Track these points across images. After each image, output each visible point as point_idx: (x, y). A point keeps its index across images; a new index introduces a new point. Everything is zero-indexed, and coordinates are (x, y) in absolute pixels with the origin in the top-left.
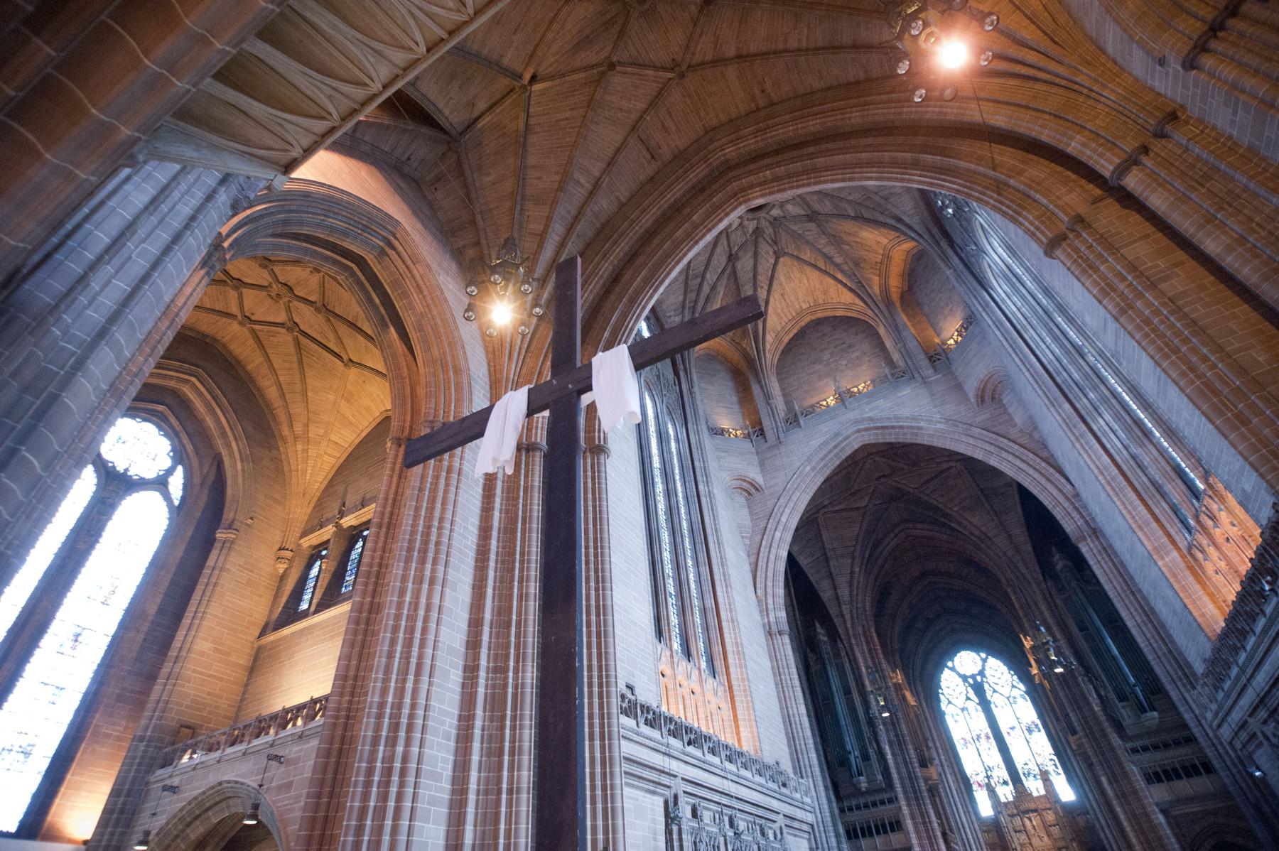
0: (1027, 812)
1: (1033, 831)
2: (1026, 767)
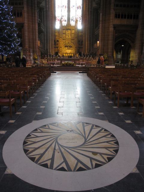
0: (68, 29)
2: (73, 18)
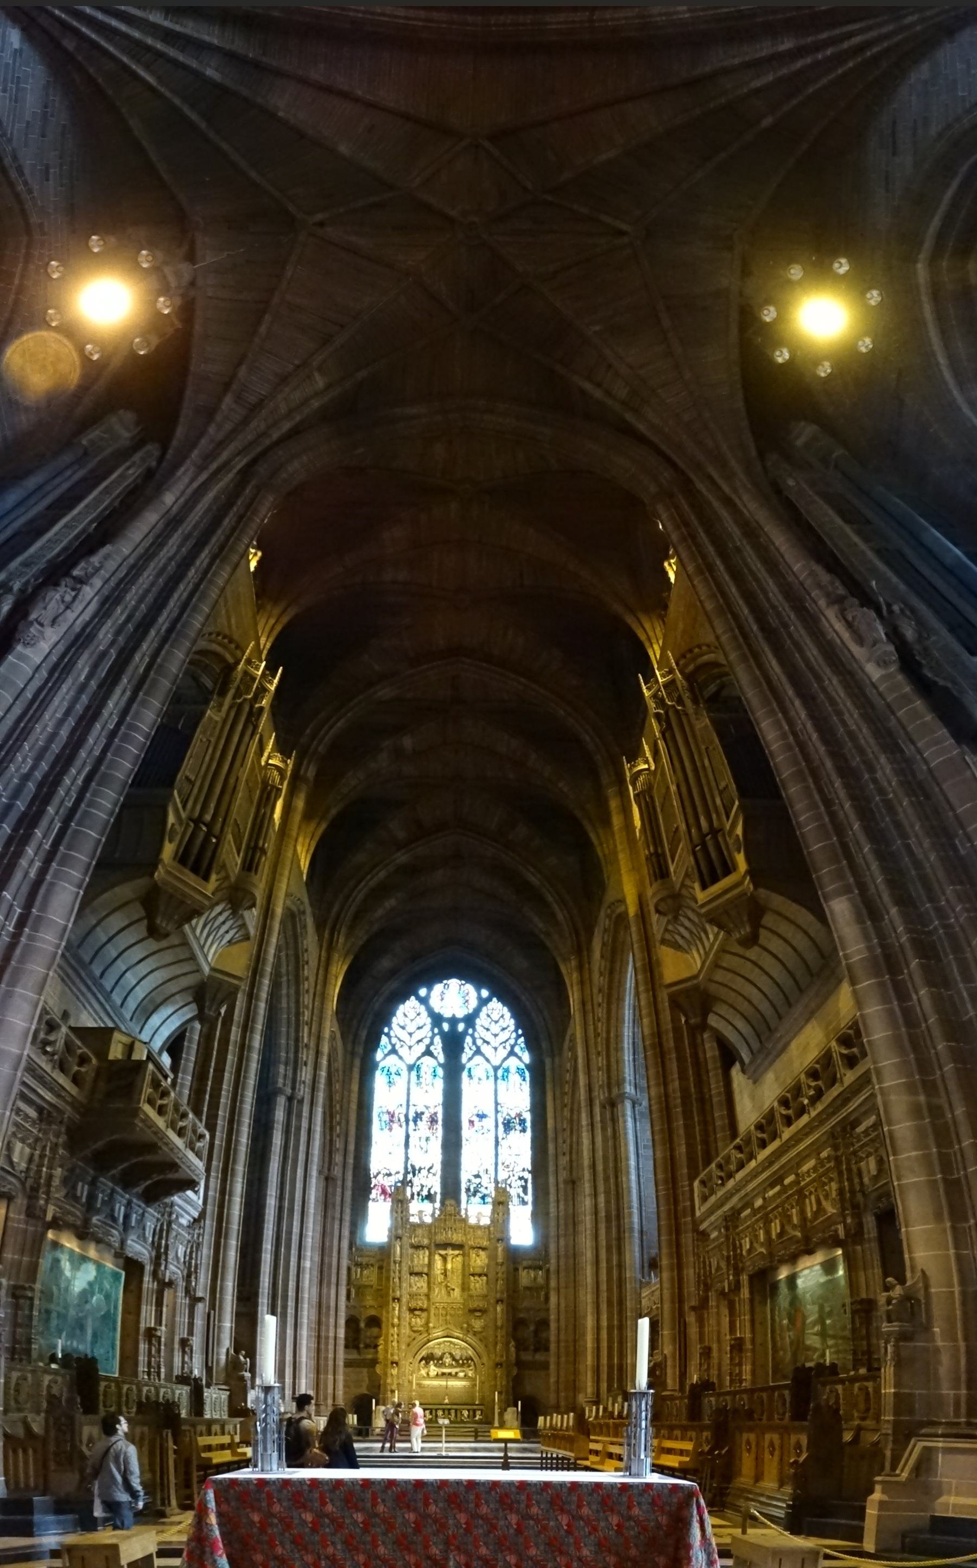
1: (440, 1278)
2: (478, 1180)
